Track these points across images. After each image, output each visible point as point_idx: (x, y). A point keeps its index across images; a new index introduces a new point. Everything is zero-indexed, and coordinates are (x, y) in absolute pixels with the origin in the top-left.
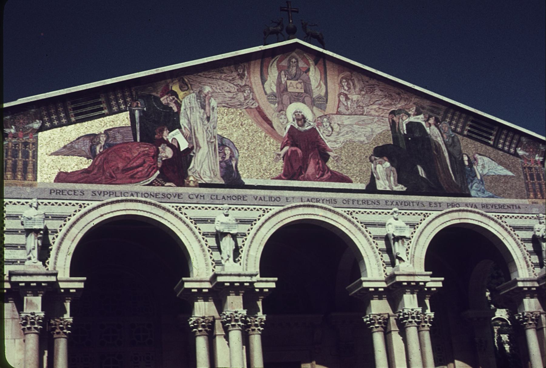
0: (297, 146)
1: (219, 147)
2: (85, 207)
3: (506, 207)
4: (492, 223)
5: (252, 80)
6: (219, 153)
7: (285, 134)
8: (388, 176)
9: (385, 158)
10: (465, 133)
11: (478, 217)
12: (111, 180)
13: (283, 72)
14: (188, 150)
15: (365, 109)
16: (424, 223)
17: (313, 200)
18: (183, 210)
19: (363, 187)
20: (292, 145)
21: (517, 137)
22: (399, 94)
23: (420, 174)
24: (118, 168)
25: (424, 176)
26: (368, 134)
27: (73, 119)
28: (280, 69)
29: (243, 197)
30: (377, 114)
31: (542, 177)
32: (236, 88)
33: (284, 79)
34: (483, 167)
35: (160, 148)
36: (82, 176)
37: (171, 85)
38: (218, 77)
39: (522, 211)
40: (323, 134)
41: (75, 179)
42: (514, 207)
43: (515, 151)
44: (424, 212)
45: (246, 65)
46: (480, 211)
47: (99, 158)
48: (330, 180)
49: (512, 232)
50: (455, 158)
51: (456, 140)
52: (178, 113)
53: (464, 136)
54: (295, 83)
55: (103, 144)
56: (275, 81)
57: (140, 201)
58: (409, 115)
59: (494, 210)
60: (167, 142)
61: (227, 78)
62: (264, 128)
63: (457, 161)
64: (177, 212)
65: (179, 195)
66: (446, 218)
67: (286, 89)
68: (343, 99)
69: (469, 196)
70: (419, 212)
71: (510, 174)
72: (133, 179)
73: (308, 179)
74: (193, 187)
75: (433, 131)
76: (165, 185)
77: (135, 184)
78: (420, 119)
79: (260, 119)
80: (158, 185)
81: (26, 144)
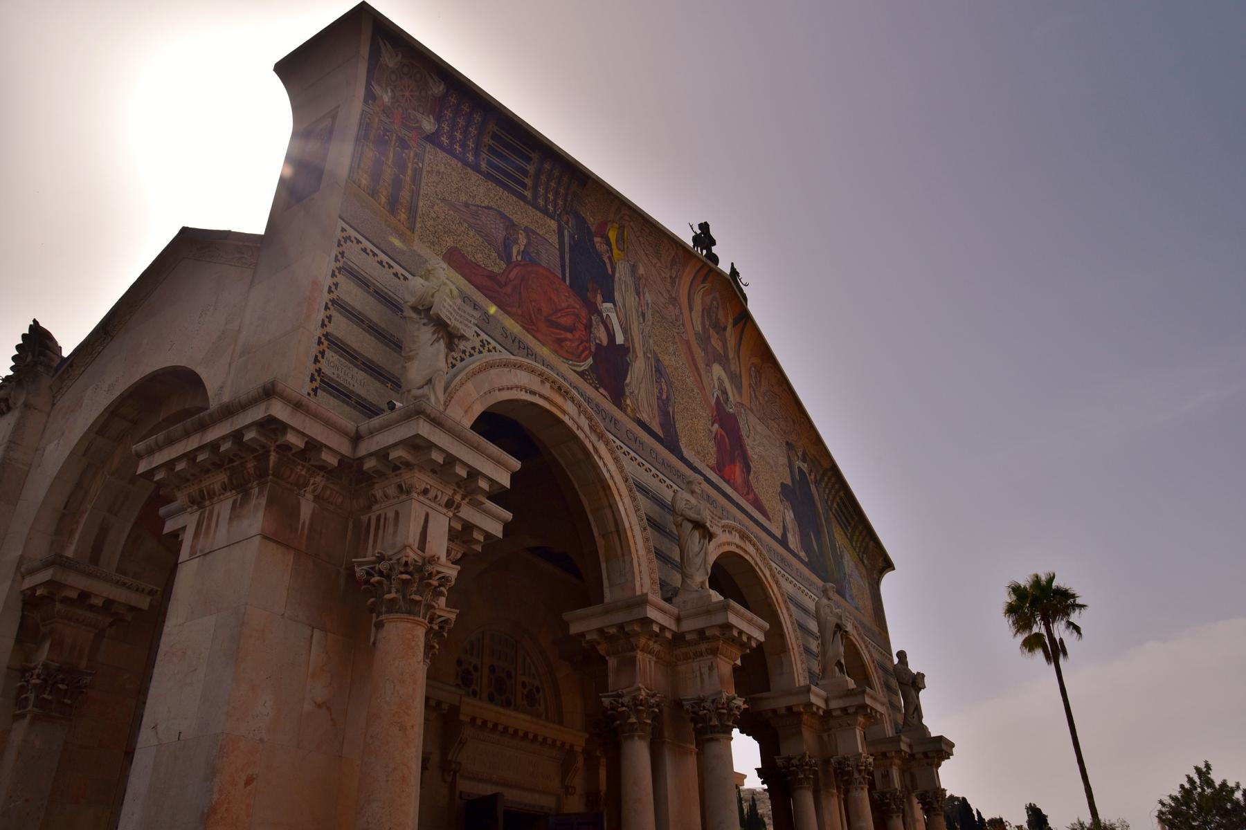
1: (655, 371)
2: (489, 351)
6: (656, 381)
7: (713, 402)
10: (834, 511)
19: (779, 534)
24: (540, 310)
25: (817, 550)
27: (484, 166)
35: (593, 317)
37: (609, 226)
38: (654, 262)
43: (863, 557)
47: (515, 271)
57: (572, 399)
60: (600, 314)
61: (662, 272)
74: (630, 417)
76: (600, 390)
77: (562, 359)
80: (590, 384)
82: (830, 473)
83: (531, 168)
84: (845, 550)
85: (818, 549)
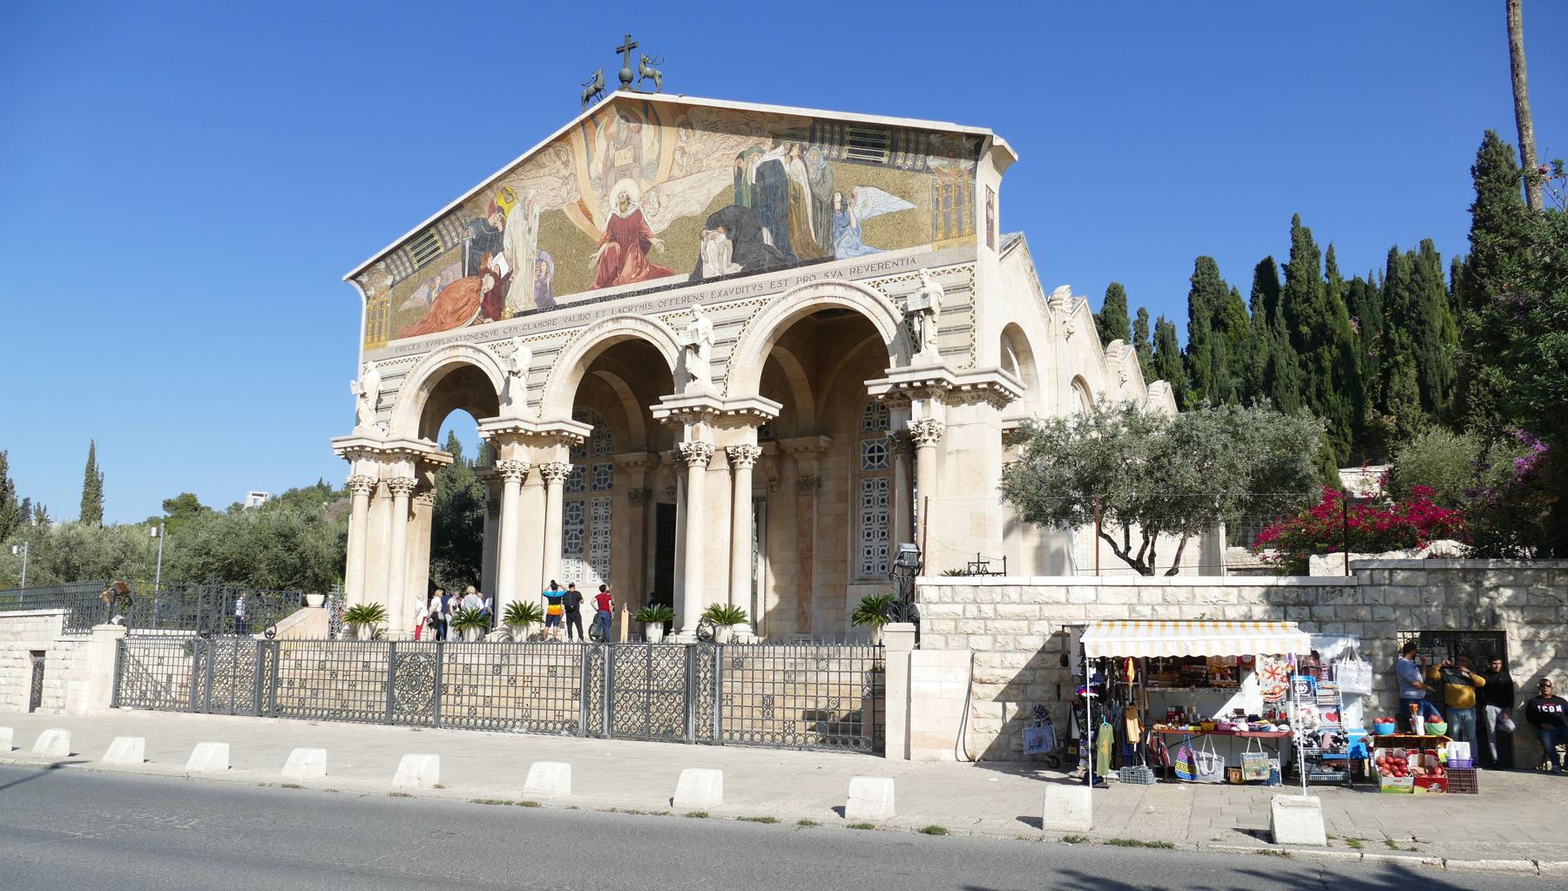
0: (615, 240)
3: (891, 264)
4: (859, 296)
5: (578, 164)
7: (603, 227)
8: (720, 255)
9: (721, 229)
11: (840, 291)
13: (612, 143)
14: (509, 275)
15: (705, 162)
16: (758, 313)
17: (626, 310)
18: (497, 349)
19: (685, 278)
20: (611, 241)
21: (922, 138)
22: (747, 124)
23: (765, 241)
26: (702, 199)
28: (608, 138)
29: (553, 322)
30: (719, 164)
31: (966, 199)
32: (561, 181)
33: (612, 150)
34: (865, 205)
36: (419, 328)
39: (915, 266)
41: (413, 333)
42: (905, 262)
44: (761, 298)
45: (568, 147)
46: (841, 281)
48: (648, 277)
49: (891, 307)
50: (821, 202)
51: (827, 172)
52: (503, 233)
53: (843, 161)
54: (622, 152)
55: (437, 287)
56: (602, 158)
57: (461, 346)
58: (762, 152)
59: (869, 274)
62: (581, 224)
63: (823, 207)
64: (491, 353)
65: (495, 332)
66: (792, 300)
67: (613, 164)
68: (678, 155)
69: (832, 259)
70: (753, 300)
71: (907, 205)
72: (459, 321)
73: (624, 282)
78: (778, 154)
79: (581, 214)
81: (382, 303)
82: (818, 127)
83: (436, 237)
84: (858, 190)
85: (776, 236)
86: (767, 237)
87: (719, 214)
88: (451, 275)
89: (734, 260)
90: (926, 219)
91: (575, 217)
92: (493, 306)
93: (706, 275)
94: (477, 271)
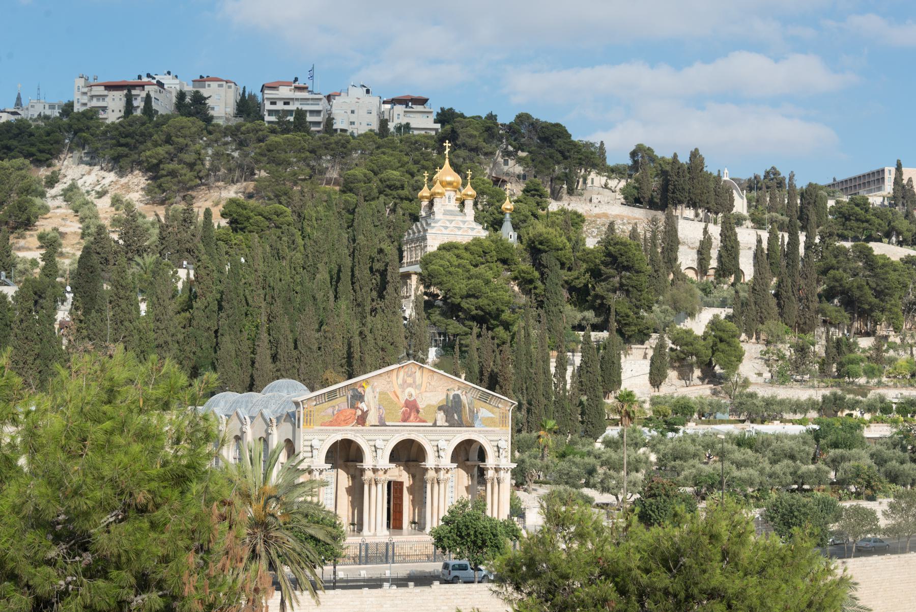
7: (403, 402)
12: (339, 425)
14: (367, 411)
19: (431, 424)
20: (407, 407)
28: (404, 372)
29: (385, 430)
40: (418, 402)
48: (419, 422)
63: (472, 411)
71: (493, 416)
72: (347, 424)
75: (463, 398)
86: (456, 417)
87: (442, 406)
88: (343, 407)
89: (446, 421)
90: (497, 420)
91: (392, 396)
92: (362, 420)
93: (438, 424)
94: (353, 406)
